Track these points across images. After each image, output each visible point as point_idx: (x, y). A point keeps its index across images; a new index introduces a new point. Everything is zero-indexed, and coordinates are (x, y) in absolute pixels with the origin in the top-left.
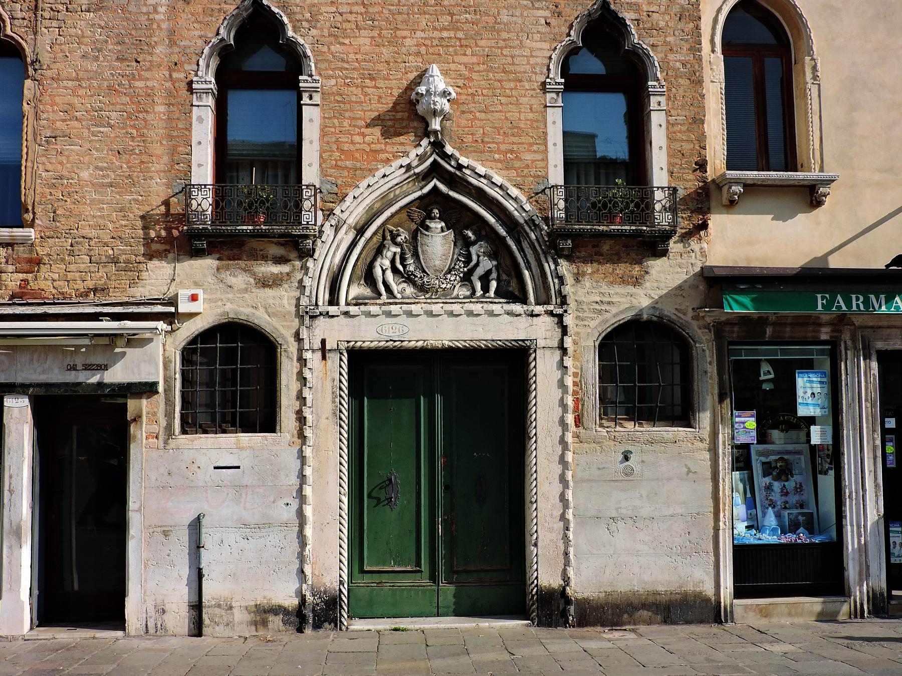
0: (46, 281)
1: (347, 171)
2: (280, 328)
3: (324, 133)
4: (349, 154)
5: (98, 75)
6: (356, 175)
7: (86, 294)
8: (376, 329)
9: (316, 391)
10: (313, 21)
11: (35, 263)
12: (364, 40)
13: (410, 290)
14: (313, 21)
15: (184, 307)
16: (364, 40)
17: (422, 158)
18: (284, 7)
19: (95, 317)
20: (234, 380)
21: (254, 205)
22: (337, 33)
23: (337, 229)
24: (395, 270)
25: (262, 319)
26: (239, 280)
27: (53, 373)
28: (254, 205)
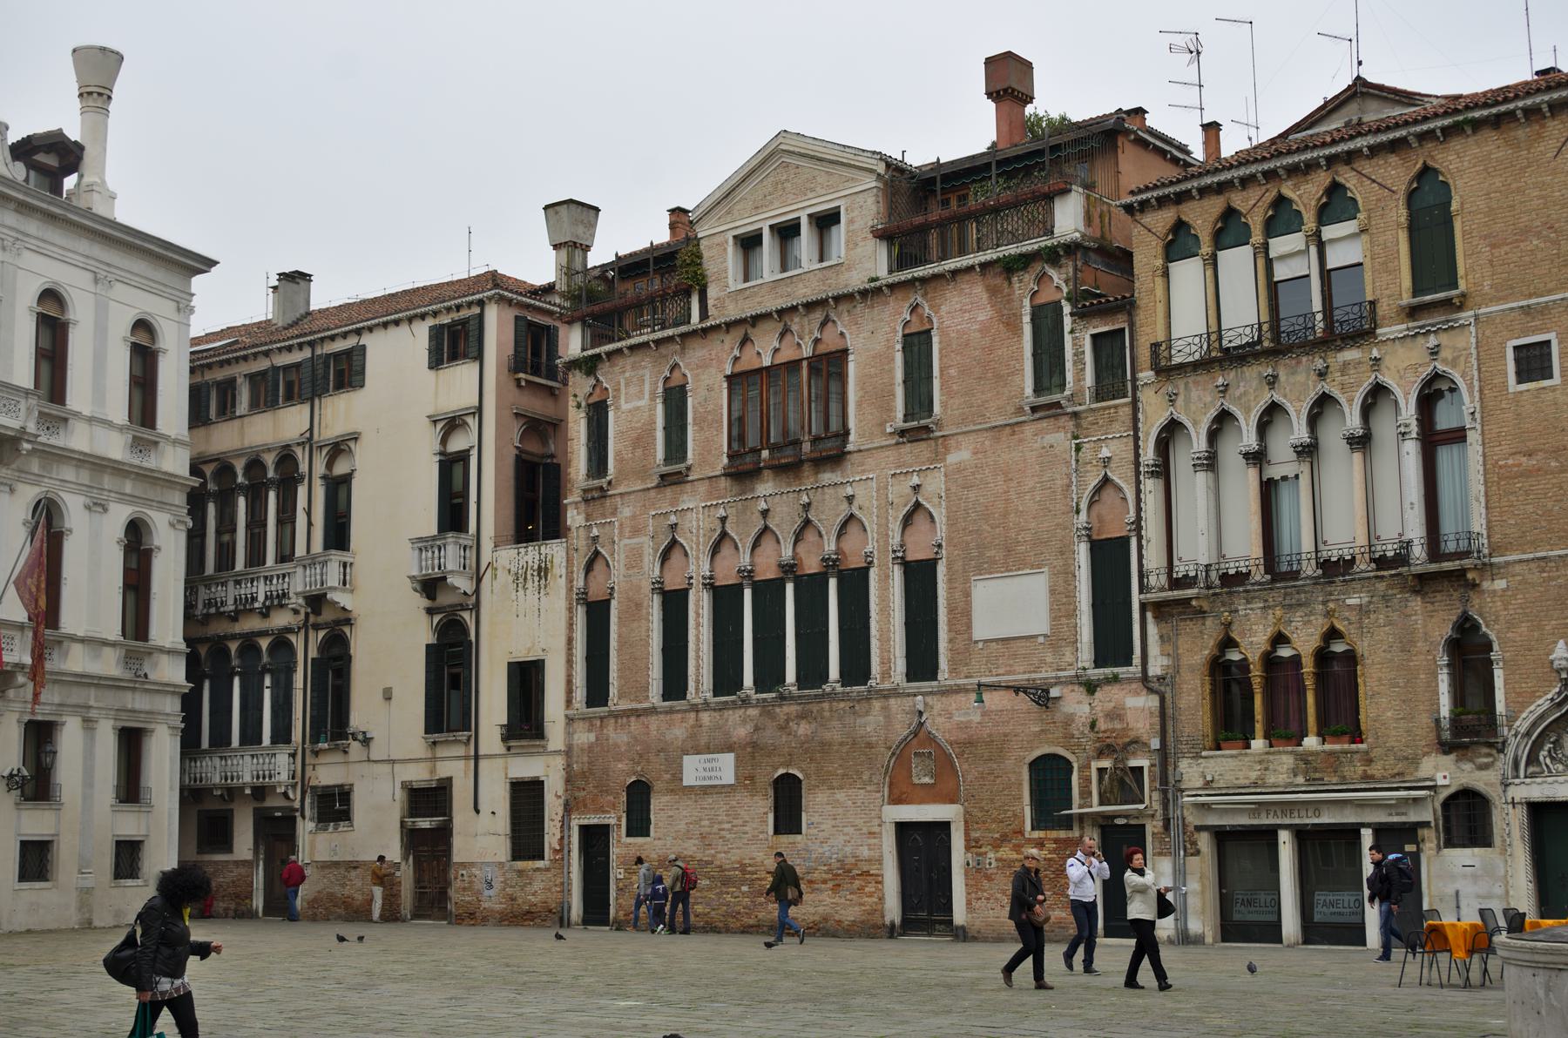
0: (1376, 770)
1: (1519, 702)
2: (1493, 793)
3: (1506, 684)
4: (1519, 694)
5: (1391, 660)
6: (1524, 705)
7: (1394, 776)
8: (1539, 791)
9: (1510, 824)
10: (1496, 621)
11: (1370, 761)
12: (1524, 628)
13: (1561, 767)
14: (1496, 621)
15: (1441, 782)
16: (1524, 628)
17: (1559, 693)
18: (1481, 615)
19: (1397, 789)
20: (1467, 819)
21: (1472, 729)
22: (1511, 625)
23: (1516, 735)
24: (1552, 759)
25: (1480, 786)
26: (1468, 766)
27: (1382, 817)
28: (1472, 729)
